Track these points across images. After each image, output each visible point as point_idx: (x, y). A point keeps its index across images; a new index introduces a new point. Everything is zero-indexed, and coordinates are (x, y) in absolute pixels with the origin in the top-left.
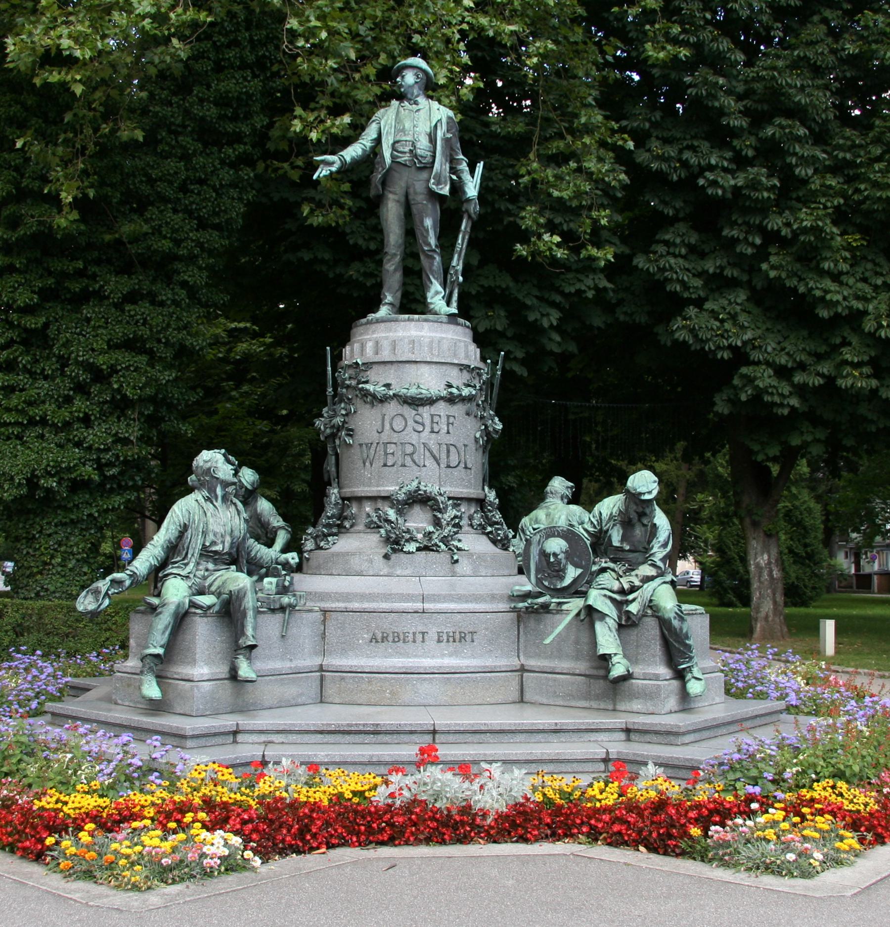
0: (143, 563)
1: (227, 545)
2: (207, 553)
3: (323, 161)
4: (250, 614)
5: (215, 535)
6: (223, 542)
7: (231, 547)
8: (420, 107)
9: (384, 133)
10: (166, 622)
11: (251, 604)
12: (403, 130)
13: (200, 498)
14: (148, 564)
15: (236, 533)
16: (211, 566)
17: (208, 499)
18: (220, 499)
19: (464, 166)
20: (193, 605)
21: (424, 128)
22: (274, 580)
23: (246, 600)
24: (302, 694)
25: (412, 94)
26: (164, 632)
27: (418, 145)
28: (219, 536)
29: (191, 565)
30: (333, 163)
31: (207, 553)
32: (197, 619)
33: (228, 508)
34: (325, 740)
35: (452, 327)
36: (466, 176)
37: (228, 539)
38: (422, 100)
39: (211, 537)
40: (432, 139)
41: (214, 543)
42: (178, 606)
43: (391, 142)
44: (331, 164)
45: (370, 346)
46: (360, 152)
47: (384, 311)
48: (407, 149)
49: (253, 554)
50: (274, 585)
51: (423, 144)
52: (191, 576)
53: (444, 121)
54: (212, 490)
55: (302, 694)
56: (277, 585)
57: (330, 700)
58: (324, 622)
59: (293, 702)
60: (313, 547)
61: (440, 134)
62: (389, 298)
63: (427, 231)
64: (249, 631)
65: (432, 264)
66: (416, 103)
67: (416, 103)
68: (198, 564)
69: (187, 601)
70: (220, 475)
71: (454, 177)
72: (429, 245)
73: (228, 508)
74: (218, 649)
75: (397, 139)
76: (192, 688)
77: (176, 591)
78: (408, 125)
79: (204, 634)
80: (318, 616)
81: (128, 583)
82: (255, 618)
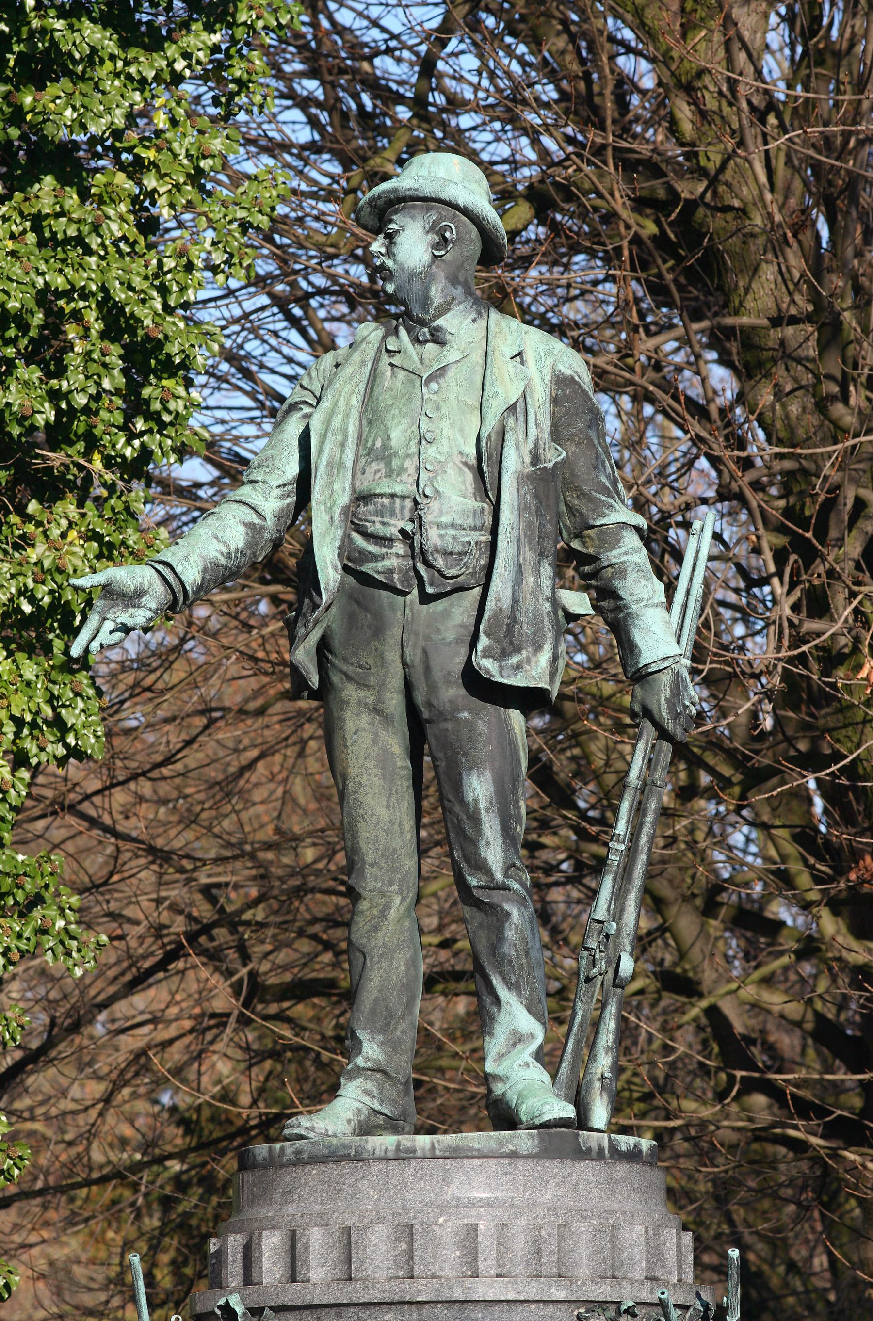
3: (108, 591)
8: (451, 355)
9: (320, 463)
12: (385, 455)
19: (631, 552)
21: (455, 439)
25: (426, 301)
27: (432, 513)
30: (139, 593)
35: (554, 1167)
36: (641, 589)
38: (459, 323)
40: (485, 475)
43: (343, 499)
44: (131, 598)
45: (271, 1243)
46: (237, 538)
47: (353, 1099)
48: (394, 526)
51: (453, 504)
53: (540, 395)
61: (514, 462)
62: (371, 1049)
63: (475, 819)
65: (499, 937)
66: (438, 338)
67: (438, 338)
71: (578, 602)
72: (482, 867)
75: (364, 484)
78: (398, 434)
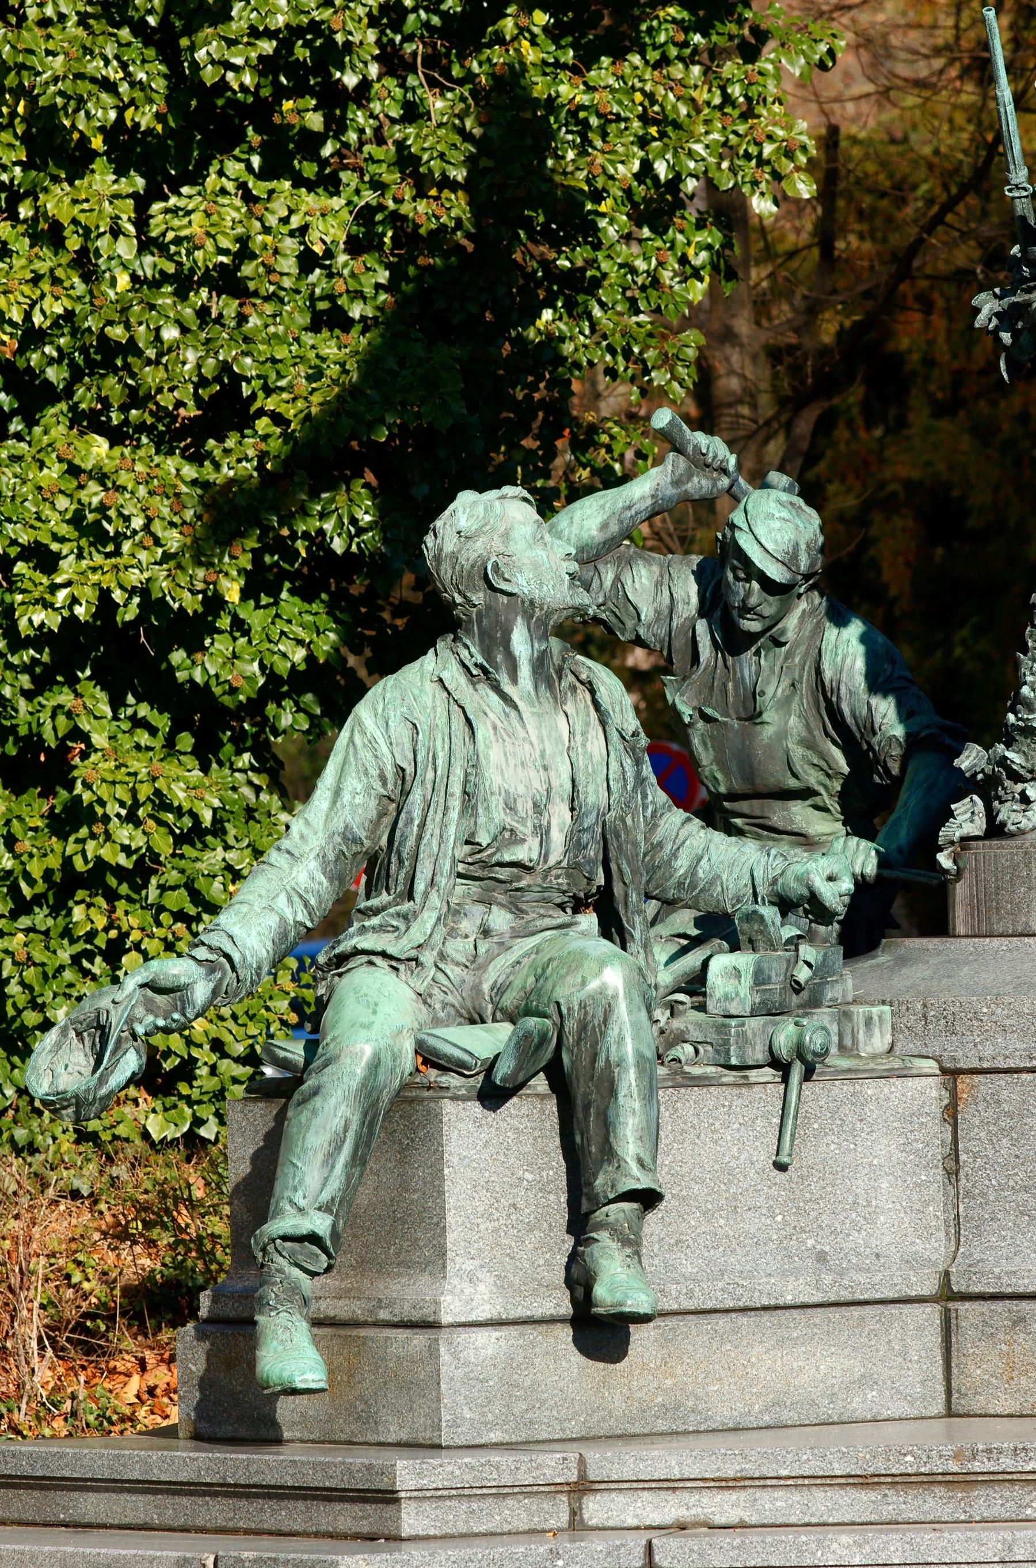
0: (254, 922)
1: (558, 839)
2: (489, 873)
4: (629, 1081)
5: (510, 807)
6: (543, 833)
7: (574, 844)
10: (336, 1123)
11: (629, 1048)
13: (454, 676)
14: (272, 921)
15: (594, 795)
16: (500, 919)
17: (483, 675)
18: (525, 671)
20: (429, 1057)
22: (744, 960)
23: (613, 1033)
24: (865, 1381)
26: (330, 1159)
28: (525, 807)
29: (428, 918)
31: (489, 873)
32: (449, 1108)
33: (559, 701)
34: (888, 1512)
37: (560, 817)
39: (492, 817)
41: (510, 836)
42: (375, 1065)
49: (682, 865)
50: (747, 980)
52: (428, 957)
54: (495, 641)
55: (865, 1381)
56: (760, 978)
57: (978, 1404)
58: (951, 1113)
59: (827, 1410)
60: (977, 826)
64: (629, 1144)
68: (454, 912)
69: (408, 1046)
70: (522, 583)
73: (559, 701)
74: (528, 1214)
76: (433, 1353)
77: (377, 1017)
79: (493, 1167)
80: (929, 1091)
81: (201, 992)
82: (650, 1092)
